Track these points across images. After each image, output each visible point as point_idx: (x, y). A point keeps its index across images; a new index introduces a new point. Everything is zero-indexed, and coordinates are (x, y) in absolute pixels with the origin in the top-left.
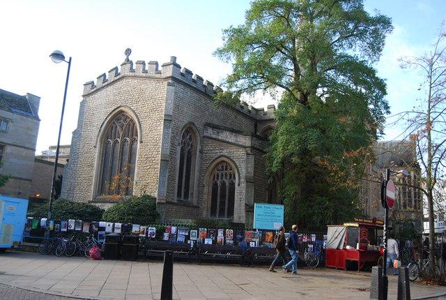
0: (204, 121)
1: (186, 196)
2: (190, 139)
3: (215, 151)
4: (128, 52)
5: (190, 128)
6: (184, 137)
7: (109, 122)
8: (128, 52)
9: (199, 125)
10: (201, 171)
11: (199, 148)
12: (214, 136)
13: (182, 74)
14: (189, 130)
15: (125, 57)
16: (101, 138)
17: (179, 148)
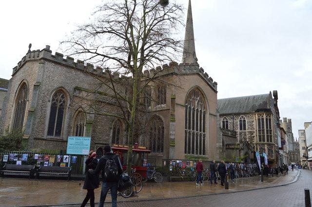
0: (74, 86)
1: (58, 133)
2: (63, 97)
3: (77, 103)
4: (30, 46)
5: (61, 90)
6: (55, 95)
7: (20, 89)
8: (30, 46)
9: (69, 88)
10: (70, 118)
11: (69, 102)
12: (78, 95)
13: (53, 56)
14: (60, 91)
15: (28, 49)
16: (16, 100)
17: (49, 104)
